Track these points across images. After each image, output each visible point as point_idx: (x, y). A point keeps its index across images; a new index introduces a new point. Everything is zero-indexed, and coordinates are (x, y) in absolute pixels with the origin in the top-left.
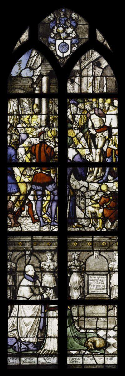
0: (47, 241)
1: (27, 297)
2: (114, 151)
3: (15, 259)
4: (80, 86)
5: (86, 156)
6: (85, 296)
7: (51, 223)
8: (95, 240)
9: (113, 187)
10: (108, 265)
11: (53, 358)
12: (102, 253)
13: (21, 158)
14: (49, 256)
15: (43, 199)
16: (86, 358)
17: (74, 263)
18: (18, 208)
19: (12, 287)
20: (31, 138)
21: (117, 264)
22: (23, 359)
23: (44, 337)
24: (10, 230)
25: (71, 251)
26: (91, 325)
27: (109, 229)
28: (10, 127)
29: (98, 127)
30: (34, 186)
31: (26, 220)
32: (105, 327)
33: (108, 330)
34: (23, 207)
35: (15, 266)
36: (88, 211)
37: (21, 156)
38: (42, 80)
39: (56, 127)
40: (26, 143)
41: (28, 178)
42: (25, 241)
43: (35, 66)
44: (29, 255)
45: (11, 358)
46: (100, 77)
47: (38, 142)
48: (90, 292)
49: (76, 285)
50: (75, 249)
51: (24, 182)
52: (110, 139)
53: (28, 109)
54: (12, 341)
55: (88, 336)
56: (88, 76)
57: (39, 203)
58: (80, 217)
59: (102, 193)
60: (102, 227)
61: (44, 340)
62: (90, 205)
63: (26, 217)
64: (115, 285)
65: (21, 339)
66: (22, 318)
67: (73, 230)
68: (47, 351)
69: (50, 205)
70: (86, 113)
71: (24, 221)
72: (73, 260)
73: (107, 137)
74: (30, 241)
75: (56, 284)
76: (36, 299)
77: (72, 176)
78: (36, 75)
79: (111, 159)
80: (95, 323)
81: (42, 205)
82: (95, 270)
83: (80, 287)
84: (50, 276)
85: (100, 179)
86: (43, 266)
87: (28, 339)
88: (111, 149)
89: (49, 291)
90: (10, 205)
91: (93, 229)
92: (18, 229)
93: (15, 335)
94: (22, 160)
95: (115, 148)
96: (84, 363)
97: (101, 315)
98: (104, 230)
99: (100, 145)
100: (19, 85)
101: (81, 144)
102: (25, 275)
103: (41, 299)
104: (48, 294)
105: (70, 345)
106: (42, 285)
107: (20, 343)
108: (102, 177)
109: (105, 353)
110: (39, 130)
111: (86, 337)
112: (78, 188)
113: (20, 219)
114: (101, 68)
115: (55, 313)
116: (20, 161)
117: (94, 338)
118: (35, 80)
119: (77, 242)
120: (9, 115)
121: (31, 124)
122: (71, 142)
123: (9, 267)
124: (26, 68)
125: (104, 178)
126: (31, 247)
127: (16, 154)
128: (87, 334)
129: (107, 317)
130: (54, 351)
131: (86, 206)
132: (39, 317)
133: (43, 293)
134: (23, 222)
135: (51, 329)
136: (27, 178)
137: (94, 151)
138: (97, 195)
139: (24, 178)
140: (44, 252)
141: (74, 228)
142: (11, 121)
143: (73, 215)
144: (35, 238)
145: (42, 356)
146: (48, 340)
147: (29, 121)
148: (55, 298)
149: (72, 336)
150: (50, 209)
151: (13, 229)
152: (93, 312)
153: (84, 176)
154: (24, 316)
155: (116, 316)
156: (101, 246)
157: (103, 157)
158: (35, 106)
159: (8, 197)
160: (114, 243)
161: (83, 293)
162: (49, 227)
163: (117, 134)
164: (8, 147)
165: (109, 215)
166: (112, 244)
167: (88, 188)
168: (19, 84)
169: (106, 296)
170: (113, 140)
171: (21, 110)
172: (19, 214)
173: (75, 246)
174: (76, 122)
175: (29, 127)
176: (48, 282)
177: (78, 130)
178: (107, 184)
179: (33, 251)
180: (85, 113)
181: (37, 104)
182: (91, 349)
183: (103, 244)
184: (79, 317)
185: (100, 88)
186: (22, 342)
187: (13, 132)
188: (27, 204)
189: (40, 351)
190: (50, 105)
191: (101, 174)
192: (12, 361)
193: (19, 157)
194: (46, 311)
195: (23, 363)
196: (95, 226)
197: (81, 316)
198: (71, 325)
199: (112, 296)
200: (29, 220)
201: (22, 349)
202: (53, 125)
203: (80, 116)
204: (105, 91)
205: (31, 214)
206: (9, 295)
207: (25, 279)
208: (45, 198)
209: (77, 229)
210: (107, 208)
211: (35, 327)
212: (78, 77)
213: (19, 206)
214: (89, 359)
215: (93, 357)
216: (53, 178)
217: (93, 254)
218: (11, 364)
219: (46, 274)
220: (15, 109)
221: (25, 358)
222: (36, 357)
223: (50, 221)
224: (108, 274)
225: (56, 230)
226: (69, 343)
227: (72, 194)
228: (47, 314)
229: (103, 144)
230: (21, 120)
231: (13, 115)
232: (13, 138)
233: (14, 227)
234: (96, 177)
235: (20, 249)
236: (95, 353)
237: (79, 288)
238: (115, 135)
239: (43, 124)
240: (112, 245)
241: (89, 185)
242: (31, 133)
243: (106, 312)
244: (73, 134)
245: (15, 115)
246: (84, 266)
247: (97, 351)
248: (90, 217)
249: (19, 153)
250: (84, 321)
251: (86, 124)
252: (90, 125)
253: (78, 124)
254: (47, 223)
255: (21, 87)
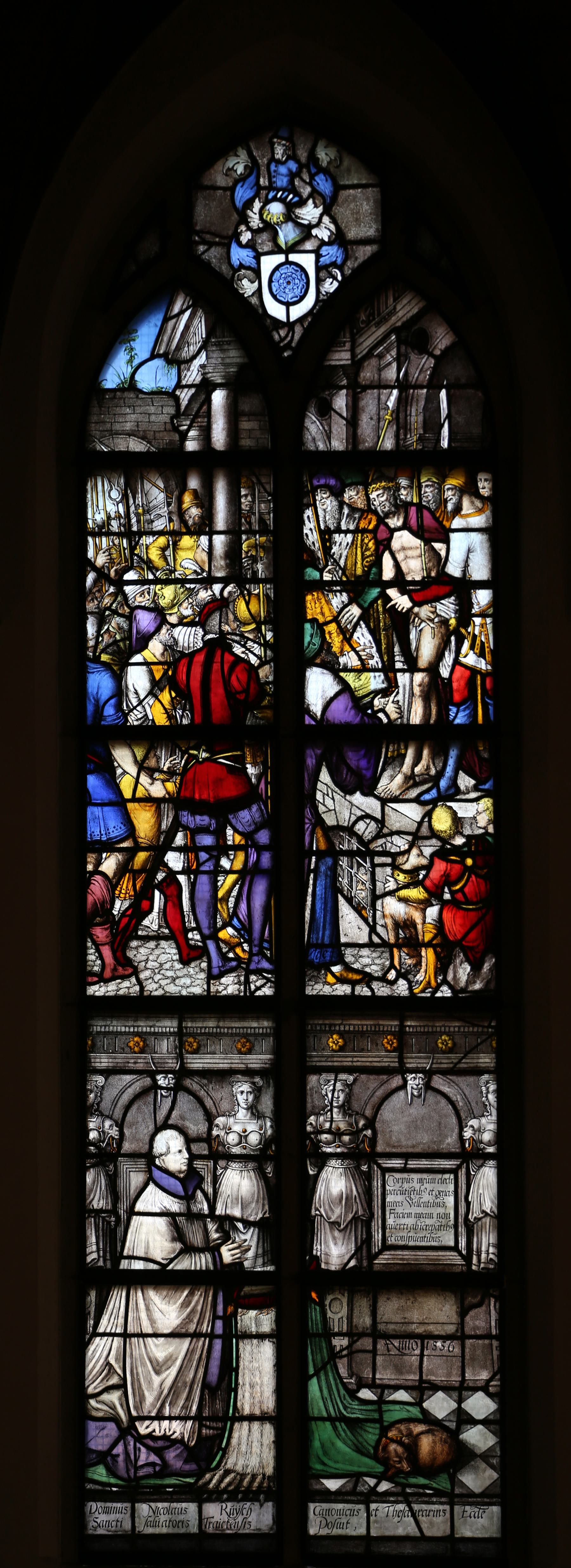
0: (236, 1035)
1: (159, 1259)
2: (479, 677)
3: (115, 1103)
4: (353, 422)
5: (373, 699)
6: (373, 1257)
7: (250, 960)
8: (410, 1027)
9: (475, 818)
10: (461, 1129)
11: (257, 1504)
12: (438, 1082)
13: (135, 708)
14: (245, 1094)
15: (217, 864)
16: (381, 1509)
17: (332, 1121)
18: (127, 904)
19: (103, 1218)
20: (174, 626)
21: (492, 1127)
22: (144, 1509)
23: (225, 1418)
24: (97, 994)
25: (319, 1071)
26: (399, 1369)
27: (464, 990)
28: (95, 582)
29: (418, 578)
30: (185, 813)
31: (157, 952)
32: (453, 1379)
33: (465, 1393)
34: (147, 899)
35: (114, 1132)
36: (384, 916)
37: (135, 702)
38: (208, 401)
39: (264, 581)
40: (155, 649)
41: (163, 781)
42: (154, 1034)
43: (186, 349)
44: (167, 1089)
45: (99, 1504)
46: (425, 391)
47: (200, 644)
48: (391, 1241)
49: (337, 1213)
50: (336, 1064)
51: (148, 799)
52: (463, 631)
53: (164, 511)
54: (105, 1432)
55: (389, 1418)
56: (381, 386)
57: (204, 881)
58: (355, 941)
59: (434, 841)
60: (436, 981)
61: (223, 1429)
62: (391, 893)
63: (158, 938)
64: (487, 1214)
65: (137, 1424)
66: (141, 1340)
67: (327, 990)
68: (235, 1478)
69: (246, 889)
70: (374, 523)
71: (151, 958)
72: (327, 1106)
73: (453, 622)
74: (171, 1034)
75: (267, 1207)
76: (193, 1268)
77: (325, 776)
78: (189, 383)
79: (467, 712)
80: (415, 1360)
81: (215, 888)
82: (410, 1150)
83: (354, 1218)
84: (245, 1174)
85: (426, 786)
86: (222, 1133)
87: (165, 1424)
88: (468, 673)
89: (243, 1237)
90: (97, 888)
91: (402, 987)
92: (128, 988)
93: (113, 1408)
94: (139, 716)
95: (482, 665)
96: (373, 1533)
97: (439, 1327)
98: (445, 992)
99: (427, 650)
100: (129, 419)
101: (354, 649)
102: (157, 1174)
103: (211, 1267)
104: (239, 1247)
105: (320, 1453)
106: (218, 1212)
107: (132, 1443)
108: (436, 785)
109: (453, 1489)
110: (204, 595)
111: (380, 1421)
112: (346, 824)
113: (137, 948)
114: (431, 355)
115: (266, 1321)
116: (134, 719)
117: (412, 1426)
118: (184, 403)
119: (341, 1034)
120: (94, 534)
121: (175, 570)
122: (317, 641)
123: (93, 1135)
124: (153, 356)
125: (443, 783)
126: (177, 1059)
127: (120, 692)
128: (385, 1407)
129: (460, 1336)
130: (264, 1475)
131: (375, 897)
132: (205, 1335)
133: (221, 1245)
134: (147, 961)
135: (252, 1386)
136: (158, 784)
137: (403, 679)
138: (415, 851)
139: (150, 781)
140: (223, 1076)
141: (331, 985)
142: (101, 560)
143: (327, 933)
144: (193, 1020)
145: (217, 1495)
146: (241, 1431)
147: (165, 558)
148: (264, 1265)
149: (325, 1414)
150: (243, 906)
151: (109, 989)
152: (406, 1316)
153: (368, 774)
154: (148, 1330)
155: (494, 1332)
156: (435, 1050)
157: (438, 705)
158: (187, 499)
159: (91, 858)
160: (482, 1042)
161: (364, 1247)
162: (242, 978)
163: (491, 611)
164: (89, 664)
165: (463, 931)
166: (475, 1044)
167: (381, 822)
168: (128, 418)
169: (454, 1259)
170: (477, 632)
171: (137, 515)
172: (132, 925)
173: (333, 1050)
174: (335, 560)
175: (167, 582)
176: (237, 1199)
177: (344, 594)
178: (454, 805)
179: (183, 1073)
180: (371, 527)
181: (195, 491)
182: (400, 1471)
183: (440, 1045)
184: (353, 1334)
185: (425, 431)
186: (140, 1438)
187: (107, 601)
188: (161, 887)
189: (208, 1476)
190: (243, 492)
191: (432, 766)
192: (102, 1518)
193: (127, 706)
194: (230, 1309)
195: (146, 1524)
196: (410, 977)
197: (361, 1330)
198: (324, 1367)
199: (475, 1260)
200: (169, 951)
201: (143, 1466)
202: (255, 573)
203: (350, 537)
204: (445, 444)
205: (176, 925)
206: (94, 1248)
207: (151, 1187)
208: (225, 863)
209: (343, 990)
210: (454, 903)
211: (191, 1376)
212: (344, 391)
213: (132, 893)
214: (391, 1514)
215: (409, 1505)
216: (253, 780)
217: (404, 1086)
218: (100, 1531)
219: (234, 1165)
220: (114, 509)
221: (153, 1505)
222: (192, 1501)
223: (246, 956)
224: (459, 1167)
225: (267, 991)
226: (317, 1444)
227: (323, 846)
228: (236, 1323)
229: (438, 648)
230: (137, 555)
231: (109, 534)
232: (106, 627)
233: (113, 979)
234: (411, 780)
235: (135, 1063)
236: (416, 1490)
237: (351, 1222)
238: (483, 615)
239: (219, 570)
240: (476, 1046)
241: (387, 808)
242: (173, 606)
243: (455, 1318)
244: (326, 610)
245: (114, 534)
246: (369, 1133)
247: (422, 1481)
248: (392, 940)
249: (131, 687)
250: (374, 1352)
251: (374, 570)
252: (388, 573)
253: (344, 570)
254: (234, 964)
255: (138, 426)
